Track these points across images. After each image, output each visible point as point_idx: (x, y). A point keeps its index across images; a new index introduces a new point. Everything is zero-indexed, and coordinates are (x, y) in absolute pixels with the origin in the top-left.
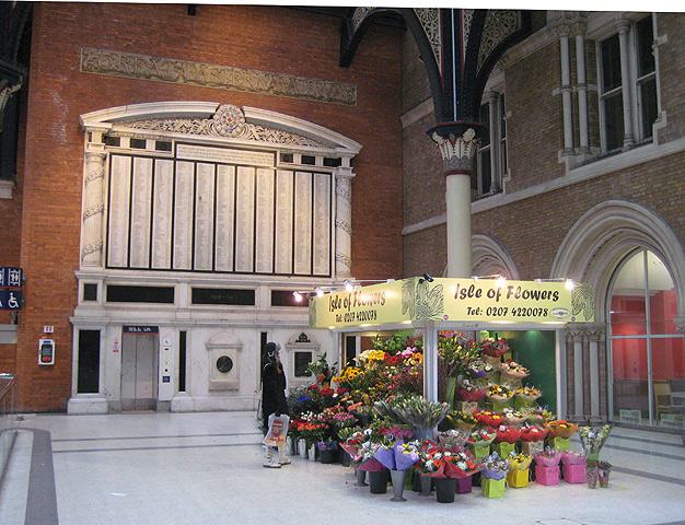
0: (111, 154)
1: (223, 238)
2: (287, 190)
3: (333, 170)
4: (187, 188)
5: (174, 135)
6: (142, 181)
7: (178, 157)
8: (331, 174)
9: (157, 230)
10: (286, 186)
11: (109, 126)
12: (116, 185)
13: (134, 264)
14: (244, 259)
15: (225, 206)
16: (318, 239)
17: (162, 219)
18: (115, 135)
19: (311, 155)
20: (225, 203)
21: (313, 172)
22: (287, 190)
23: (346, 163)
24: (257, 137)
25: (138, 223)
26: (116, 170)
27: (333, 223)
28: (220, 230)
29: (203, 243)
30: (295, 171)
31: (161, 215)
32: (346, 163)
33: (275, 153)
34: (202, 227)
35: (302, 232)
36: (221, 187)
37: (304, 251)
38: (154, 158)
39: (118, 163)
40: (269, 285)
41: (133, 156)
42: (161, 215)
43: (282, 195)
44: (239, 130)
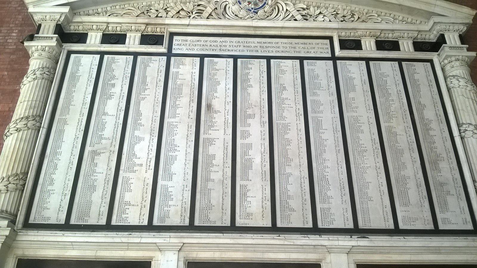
0: (70, 53)
1: (251, 167)
2: (359, 88)
3: (434, 56)
4: (186, 90)
5: (167, 21)
6: (113, 85)
7: (173, 59)
8: (431, 61)
9: (129, 159)
10: (357, 82)
11: (66, 9)
12: (70, 93)
13: (79, 218)
14: (293, 203)
15: (251, 116)
16: (435, 163)
17: (140, 139)
18: (81, 29)
19: (390, 37)
20: (250, 112)
21: (400, 61)
22: (359, 88)
23: (453, 39)
24: (299, 17)
25: (96, 147)
26: (73, 75)
27: (456, 133)
28: (245, 153)
29: (213, 176)
30: (367, 60)
31: (137, 133)
32: (453, 39)
33: (331, 39)
34: (212, 150)
35: (402, 152)
36: (243, 89)
37: (412, 185)
38: (136, 55)
39: (78, 63)
40: (349, 252)
41: (102, 54)
42: (137, 133)
43: (351, 95)
44: (267, 8)
